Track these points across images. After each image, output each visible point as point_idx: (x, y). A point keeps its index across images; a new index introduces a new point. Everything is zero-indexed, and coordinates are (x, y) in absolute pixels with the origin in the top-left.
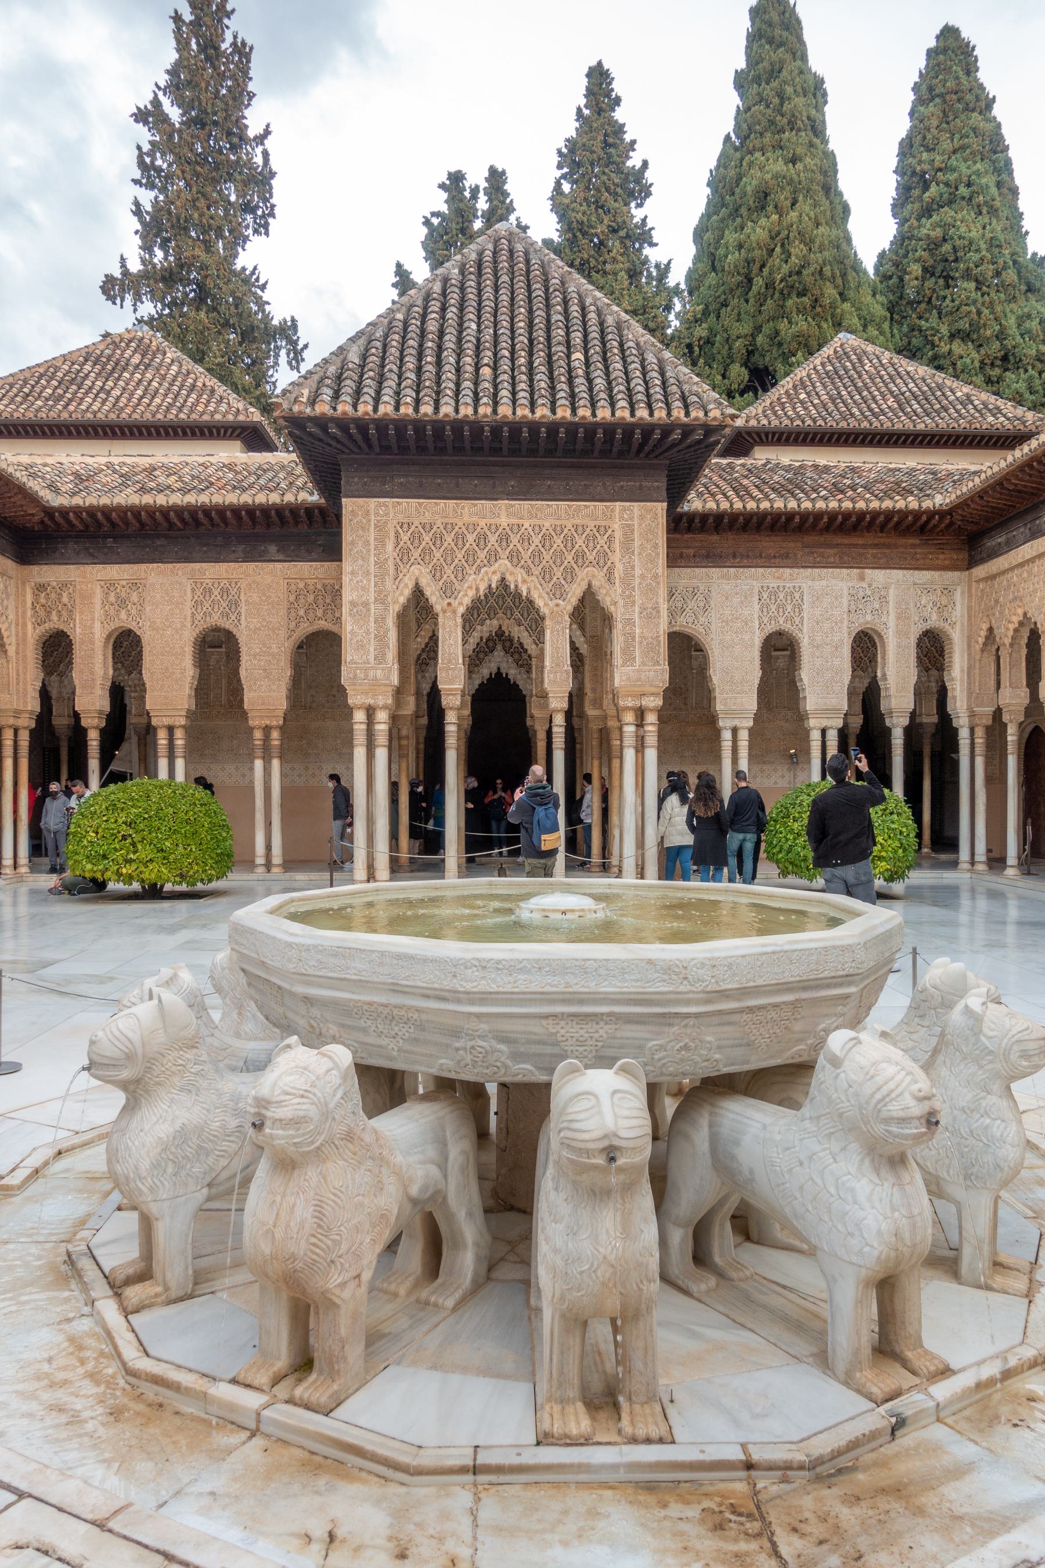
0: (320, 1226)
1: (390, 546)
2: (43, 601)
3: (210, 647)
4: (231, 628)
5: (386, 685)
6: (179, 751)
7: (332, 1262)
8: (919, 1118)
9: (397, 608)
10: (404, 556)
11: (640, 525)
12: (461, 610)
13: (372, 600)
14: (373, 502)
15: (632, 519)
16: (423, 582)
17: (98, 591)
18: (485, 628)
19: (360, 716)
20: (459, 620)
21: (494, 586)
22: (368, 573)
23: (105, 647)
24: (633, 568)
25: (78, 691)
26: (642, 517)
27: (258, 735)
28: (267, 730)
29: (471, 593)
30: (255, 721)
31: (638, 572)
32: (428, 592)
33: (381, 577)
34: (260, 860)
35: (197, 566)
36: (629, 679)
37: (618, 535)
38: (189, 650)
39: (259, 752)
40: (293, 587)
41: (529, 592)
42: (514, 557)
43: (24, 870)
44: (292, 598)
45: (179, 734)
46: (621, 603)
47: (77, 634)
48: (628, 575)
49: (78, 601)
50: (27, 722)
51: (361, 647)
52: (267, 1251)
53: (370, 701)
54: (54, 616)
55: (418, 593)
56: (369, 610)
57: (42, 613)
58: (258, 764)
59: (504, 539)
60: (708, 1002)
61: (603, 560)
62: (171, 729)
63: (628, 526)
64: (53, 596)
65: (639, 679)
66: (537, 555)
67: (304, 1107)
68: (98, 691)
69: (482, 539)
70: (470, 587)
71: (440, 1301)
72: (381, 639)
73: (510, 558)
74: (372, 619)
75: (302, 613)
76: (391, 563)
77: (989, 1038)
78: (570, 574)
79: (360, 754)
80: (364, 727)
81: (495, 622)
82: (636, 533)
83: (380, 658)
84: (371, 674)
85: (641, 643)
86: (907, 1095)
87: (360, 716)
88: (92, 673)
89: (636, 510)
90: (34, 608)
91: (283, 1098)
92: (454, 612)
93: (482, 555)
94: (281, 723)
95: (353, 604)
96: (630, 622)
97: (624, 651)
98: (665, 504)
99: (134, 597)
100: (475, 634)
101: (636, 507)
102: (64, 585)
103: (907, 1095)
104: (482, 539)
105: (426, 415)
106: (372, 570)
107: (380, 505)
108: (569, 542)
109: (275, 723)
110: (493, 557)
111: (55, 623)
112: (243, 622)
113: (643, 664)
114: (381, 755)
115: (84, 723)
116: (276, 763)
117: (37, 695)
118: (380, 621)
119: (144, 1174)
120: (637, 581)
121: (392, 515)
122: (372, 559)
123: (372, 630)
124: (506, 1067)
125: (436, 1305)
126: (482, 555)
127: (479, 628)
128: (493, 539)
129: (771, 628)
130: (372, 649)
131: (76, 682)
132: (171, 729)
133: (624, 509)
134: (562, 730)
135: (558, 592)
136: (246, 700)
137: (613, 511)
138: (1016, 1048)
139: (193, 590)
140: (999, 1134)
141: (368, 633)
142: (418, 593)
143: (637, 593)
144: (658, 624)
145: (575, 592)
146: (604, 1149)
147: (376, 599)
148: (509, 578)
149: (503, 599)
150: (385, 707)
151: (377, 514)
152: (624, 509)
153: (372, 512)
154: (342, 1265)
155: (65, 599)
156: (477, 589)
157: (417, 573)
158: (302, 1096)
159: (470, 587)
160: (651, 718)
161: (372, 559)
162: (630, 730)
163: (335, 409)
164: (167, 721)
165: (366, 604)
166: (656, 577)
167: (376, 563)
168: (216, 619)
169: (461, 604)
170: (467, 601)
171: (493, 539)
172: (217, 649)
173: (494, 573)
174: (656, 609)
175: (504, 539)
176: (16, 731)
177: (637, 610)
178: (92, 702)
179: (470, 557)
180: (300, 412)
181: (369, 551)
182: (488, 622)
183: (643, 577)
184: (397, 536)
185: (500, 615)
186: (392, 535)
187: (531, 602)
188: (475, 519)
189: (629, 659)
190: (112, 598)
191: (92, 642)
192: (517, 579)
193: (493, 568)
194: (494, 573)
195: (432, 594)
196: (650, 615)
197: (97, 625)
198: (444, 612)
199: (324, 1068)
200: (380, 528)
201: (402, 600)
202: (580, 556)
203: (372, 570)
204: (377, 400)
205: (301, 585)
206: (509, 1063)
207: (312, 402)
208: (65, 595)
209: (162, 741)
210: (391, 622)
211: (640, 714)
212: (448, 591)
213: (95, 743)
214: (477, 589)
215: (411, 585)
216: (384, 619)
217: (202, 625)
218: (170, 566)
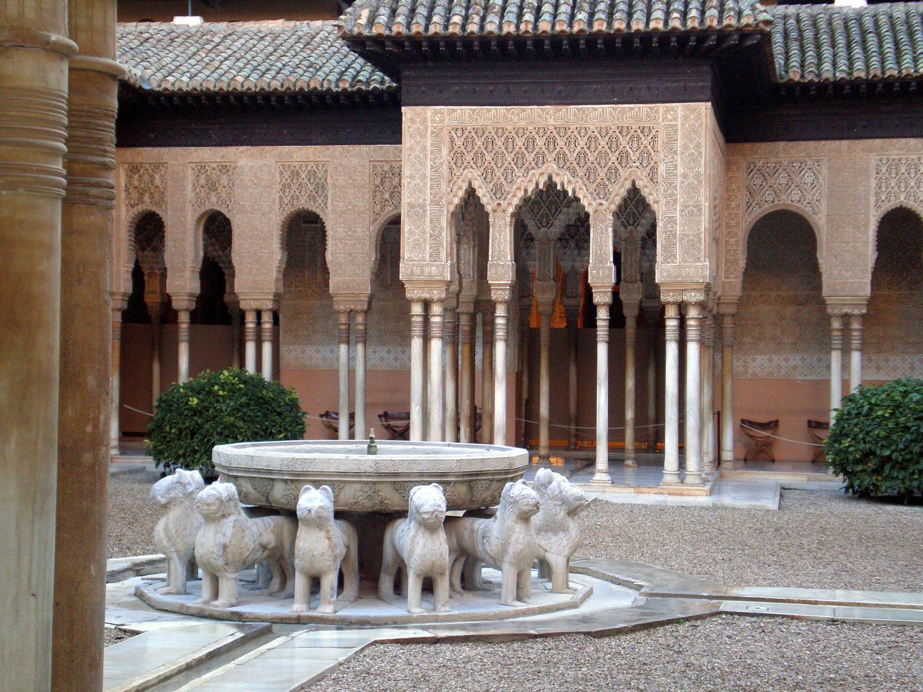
1: (445, 152)
2: (136, 183)
3: (305, 222)
4: (318, 211)
5: (440, 281)
9: (452, 208)
10: (457, 158)
11: (683, 125)
12: (511, 210)
13: (428, 202)
14: (430, 109)
15: (675, 119)
16: (476, 184)
17: (190, 172)
18: (571, 210)
19: (417, 309)
20: (508, 219)
22: (424, 176)
23: (196, 229)
24: (675, 167)
26: (686, 118)
27: (343, 319)
28: (351, 313)
29: (521, 194)
30: (341, 306)
31: (680, 171)
32: (480, 193)
33: (436, 181)
35: (286, 149)
36: (669, 275)
37: (662, 137)
40: (379, 170)
41: (574, 192)
42: (561, 159)
44: (377, 182)
46: (663, 201)
48: (671, 173)
49: (169, 182)
51: (417, 245)
53: (426, 295)
54: (147, 199)
55: (471, 192)
56: (425, 211)
57: (135, 195)
59: (551, 142)
61: (646, 158)
62: (259, 313)
63: (671, 126)
64: (146, 177)
65: (679, 275)
66: (582, 156)
68: (188, 274)
69: (530, 143)
70: (519, 188)
72: (435, 237)
73: (557, 159)
74: (428, 220)
75: (387, 196)
78: (613, 173)
79: (416, 344)
80: (420, 319)
82: (679, 133)
83: (435, 256)
84: (427, 270)
85: (681, 240)
87: (417, 309)
89: (679, 110)
90: (127, 190)
93: (530, 157)
94: (365, 307)
95: (411, 206)
96: (671, 220)
97: (664, 249)
98: (709, 104)
99: (224, 180)
100: (561, 217)
101: (679, 107)
102: (157, 166)
104: (530, 143)
105: (472, 33)
106: (428, 174)
107: (435, 113)
108: (613, 143)
109: (359, 308)
110: (540, 159)
111: (147, 205)
112: (330, 207)
113: (684, 261)
114: (436, 345)
115: (175, 305)
116: (360, 347)
117: (129, 276)
118: (435, 221)
120: (679, 180)
121: (447, 121)
122: (429, 163)
123: (428, 230)
126: (530, 157)
127: (565, 210)
128: (540, 142)
129: (892, 204)
130: (428, 248)
133: (667, 111)
134: (606, 323)
135: (601, 191)
137: (657, 112)
139: (281, 173)
141: (424, 233)
142: (471, 192)
143: (678, 192)
144: (699, 222)
145: (619, 192)
147: (432, 201)
148: (557, 180)
149: (549, 202)
150: (441, 301)
151: (433, 121)
152: (667, 111)
153: (429, 119)
155: (157, 181)
156: (526, 191)
157: (470, 176)
159: (519, 188)
160: (693, 312)
161: (429, 163)
162: (671, 324)
163: (390, 30)
164: (255, 305)
165: (422, 206)
166: (698, 175)
167: (432, 167)
168: (304, 203)
169: (509, 204)
170: (516, 201)
171: (540, 142)
172: (304, 235)
173: (542, 174)
175: (551, 142)
177: (678, 208)
178: (183, 283)
179: (519, 160)
180: (360, 34)
181: (426, 156)
183: (685, 176)
184: (452, 141)
186: (447, 139)
187: (577, 200)
188: (523, 124)
189: (670, 256)
190: (202, 181)
192: (563, 179)
193: (540, 171)
194: (542, 174)
195: (483, 194)
196: (691, 213)
197: (189, 207)
198: (495, 211)
200: (436, 134)
201: (456, 201)
202: (623, 158)
203: (428, 174)
204: (429, 19)
205: (387, 168)
207: (371, 22)
208: (157, 177)
209: (250, 325)
210: (444, 222)
211: (682, 308)
212: (498, 191)
213: (184, 326)
214: (526, 191)
215: (465, 186)
216: (439, 220)
217: (289, 210)
218: (259, 148)
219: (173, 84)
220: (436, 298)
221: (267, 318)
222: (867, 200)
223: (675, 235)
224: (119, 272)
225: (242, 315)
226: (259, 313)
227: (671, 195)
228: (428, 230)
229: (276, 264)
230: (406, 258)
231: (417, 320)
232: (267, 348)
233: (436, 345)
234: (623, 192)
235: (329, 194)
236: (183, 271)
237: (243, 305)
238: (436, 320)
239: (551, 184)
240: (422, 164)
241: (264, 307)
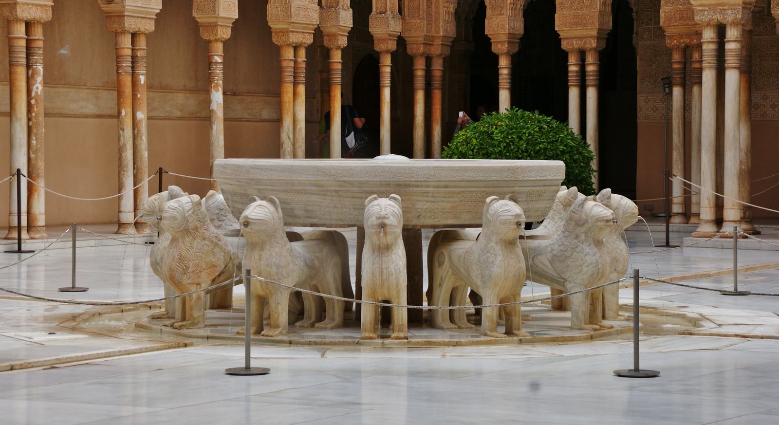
6: (591, 79)
8: (377, 226)
19: (709, 35)
25: (488, 12)
27: (676, 57)
34: (676, 208)
39: (677, 78)
45: (590, 58)
50: (436, 50)
53: (718, 17)
58: (677, 91)
60: (341, 186)
67: (174, 213)
68: (508, 12)
77: (490, 214)
80: (713, 46)
86: (374, 217)
91: (167, 209)
103: (374, 217)
117: (452, 18)
136: (662, 15)
138: (498, 219)
140: (492, 261)
150: (735, 24)
154: (190, 276)
158: (174, 209)
164: (577, 44)
176: (429, 60)
178: (503, 24)
199: (187, 201)
220: (730, 19)
221: (590, 58)
224: (437, 13)
225: (565, 55)
226: (582, 54)
231: (709, 49)
232: (592, 94)
233: (732, 78)
236: (502, 8)
237: (564, 45)
238: (731, 46)
241: (588, 46)
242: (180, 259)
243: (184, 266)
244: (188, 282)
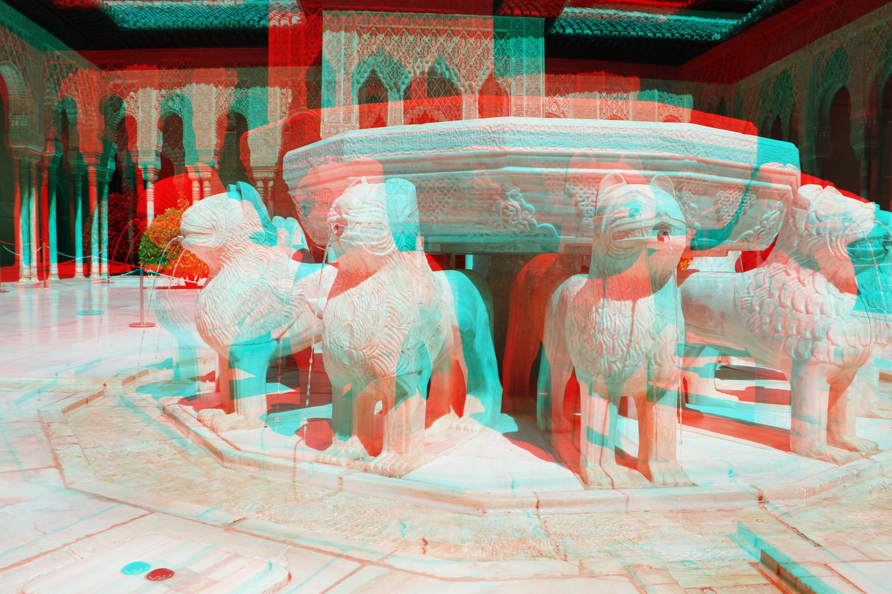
0: (393, 320)
7: (403, 352)
9: (359, 86)
12: (403, 87)
13: (342, 79)
18: (415, 112)
20: (402, 94)
21: (426, 70)
29: (411, 76)
38: (214, 126)
43: (106, 277)
47: (139, 116)
52: (346, 343)
67: (380, 214)
70: (410, 72)
71: (470, 427)
74: (342, 93)
76: (355, 54)
81: (422, 108)
88: (150, 142)
92: (399, 91)
119: (227, 322)
123: (342, 100)
124: (532, 225)
125: (466, 429)
127: (410, 111)
130: (342, 113)
131: (139, 149)
132: (201, 182)
144: (539, 100)
146: (655, 228)
147: (345, 80)
158: (378, 206)
170: (407, 81)
174: (538, 88)
177: (525, 89)
181: (340, 46)
182: (417, 108)
185: (426, 103)
187: (452, 84)
191: (150, 122)
197: (154, 111)
201: (362, 80)
206: (534, 221)
219: (144, 24)
222: (595, 111)
223: (522, 109)
227: (519, 80)
228: (342, 100)
229: (213, 147)
230: (326, 119)
234: (485, 78)
235: (250, 100)
239: (432, 71)
240: (338, 53)
241: (205, 176)
242: (393, 320)
243: (400, 335)
244: (407, 370)
